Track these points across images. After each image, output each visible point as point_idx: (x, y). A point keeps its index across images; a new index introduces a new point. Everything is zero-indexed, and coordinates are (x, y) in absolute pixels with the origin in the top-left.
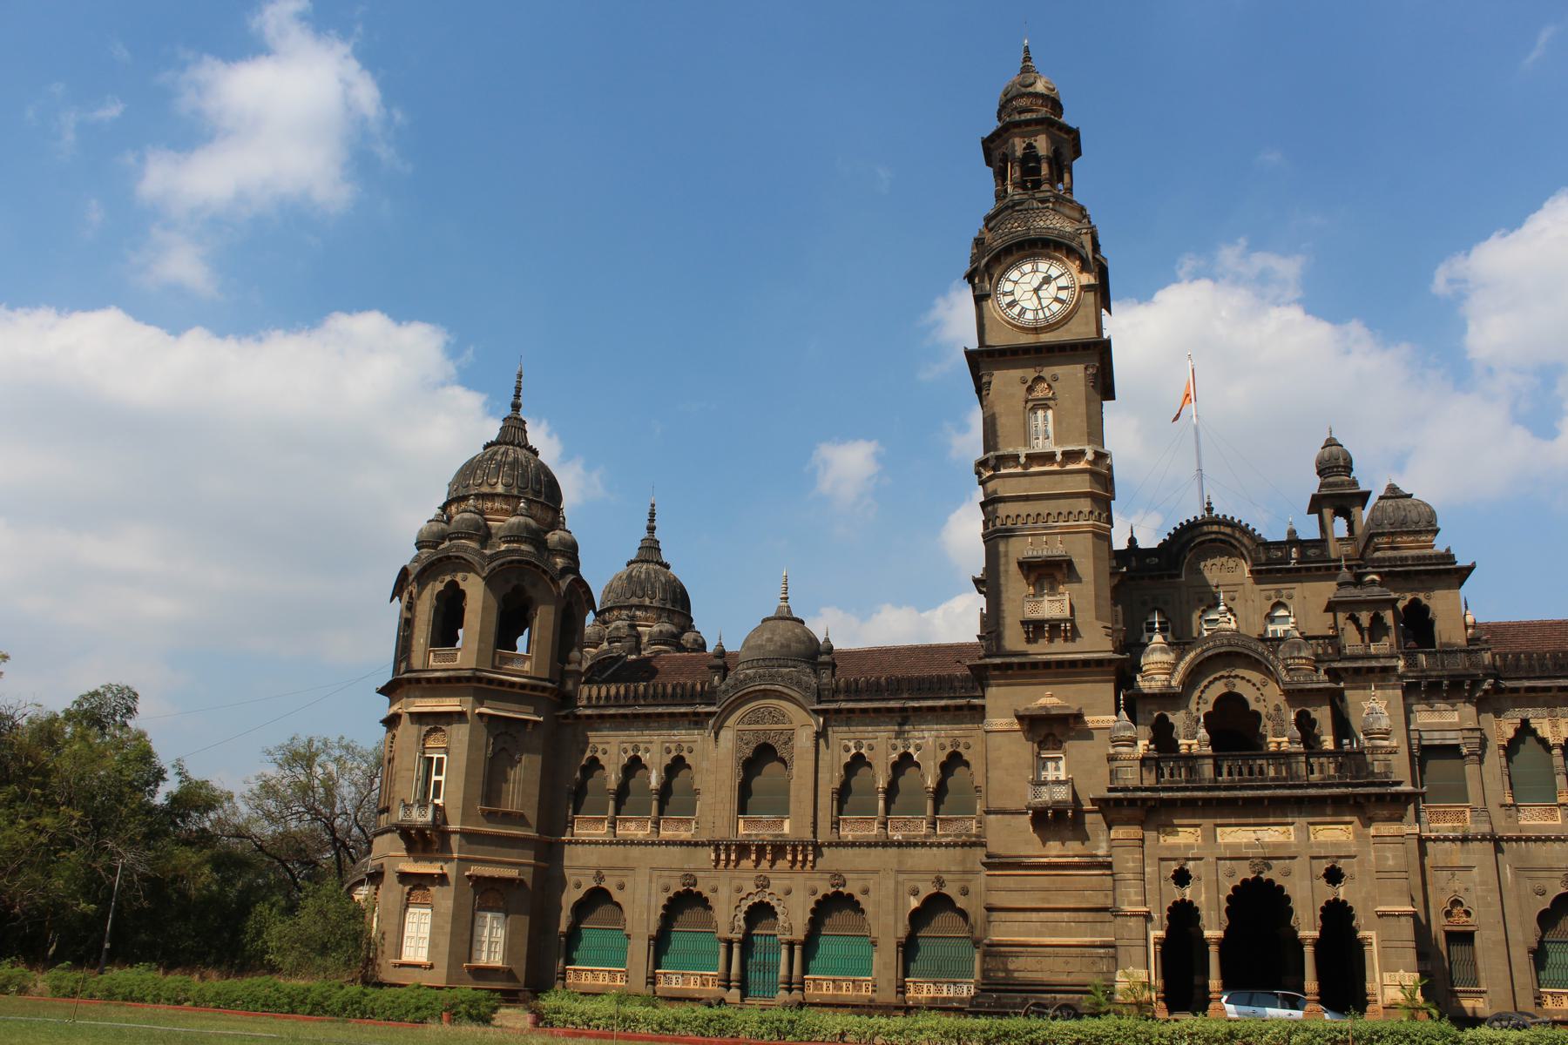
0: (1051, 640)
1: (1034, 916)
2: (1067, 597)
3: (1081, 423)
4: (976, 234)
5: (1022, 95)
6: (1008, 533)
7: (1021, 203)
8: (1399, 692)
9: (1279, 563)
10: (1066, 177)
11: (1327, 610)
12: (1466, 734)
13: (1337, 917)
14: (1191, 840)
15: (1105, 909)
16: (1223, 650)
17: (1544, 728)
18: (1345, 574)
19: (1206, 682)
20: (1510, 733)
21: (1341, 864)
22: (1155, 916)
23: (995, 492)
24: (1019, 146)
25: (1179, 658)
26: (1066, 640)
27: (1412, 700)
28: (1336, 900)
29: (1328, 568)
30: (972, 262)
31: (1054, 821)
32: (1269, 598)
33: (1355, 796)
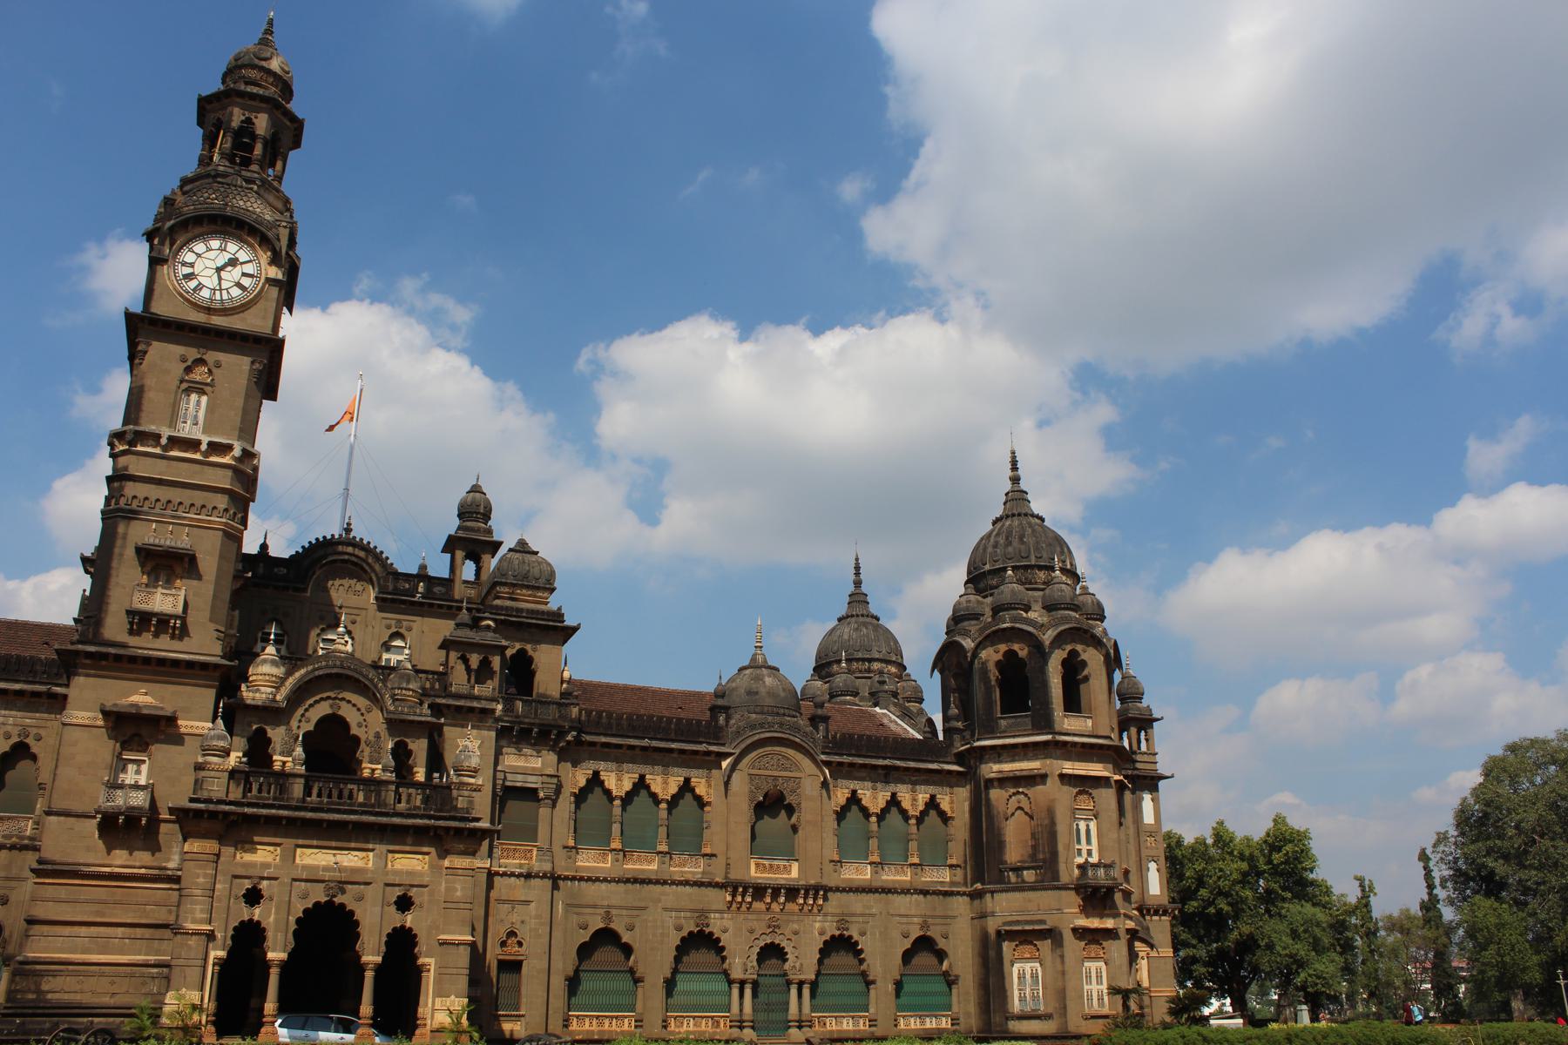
0: (156, 635)
1: (83, 930)
2: (183, 593)
3: (235, 417)
4: (168, 193)
5: (254, 67)
6: (131, 515)
7: (225, 175)
8: (493, 734)
9: (406, 595)
10: (279, 164)
11: (441, 647)
12: (546, 779)
13: (402, 944)
14: (269, 859)
15: (166, 926)
16: (334, 671)
17: (610, 781)
18: (464, 616)
19: (311, 701)
20: (582, 782)
21: (413, 892)
22: (219, 935)
23: (126, 468)
24: (237, 117)
25: (289, 673)
26: (173, 637)
27: (503, 742)
28: (403, 927)
29: (450, 607)
30: (156, 221)
31: (122, 828)
32: (389, 627)
33: (436, 828)
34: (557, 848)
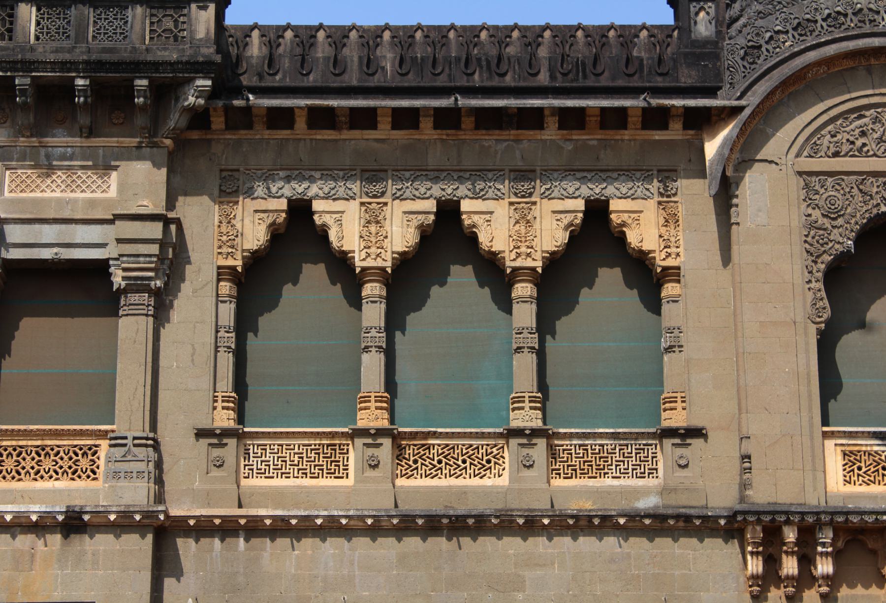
20: (255, 235)
34: (176, 435)
